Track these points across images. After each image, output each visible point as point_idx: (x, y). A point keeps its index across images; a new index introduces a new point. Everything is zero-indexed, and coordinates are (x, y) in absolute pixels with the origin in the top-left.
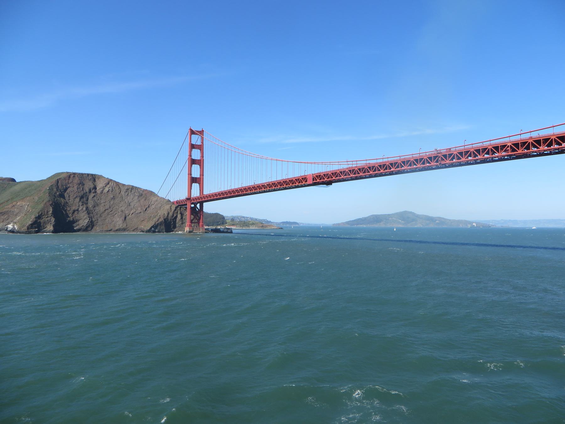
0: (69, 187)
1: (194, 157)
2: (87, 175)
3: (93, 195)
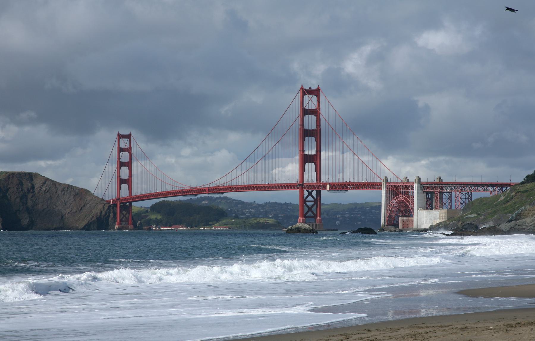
0: (9, 188)
1: (122, 160)
2: (24, 174)
3: (32, 195)
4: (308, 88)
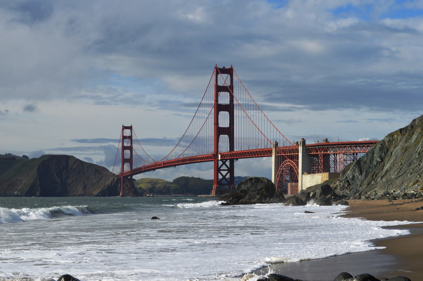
4: (222, 68)
